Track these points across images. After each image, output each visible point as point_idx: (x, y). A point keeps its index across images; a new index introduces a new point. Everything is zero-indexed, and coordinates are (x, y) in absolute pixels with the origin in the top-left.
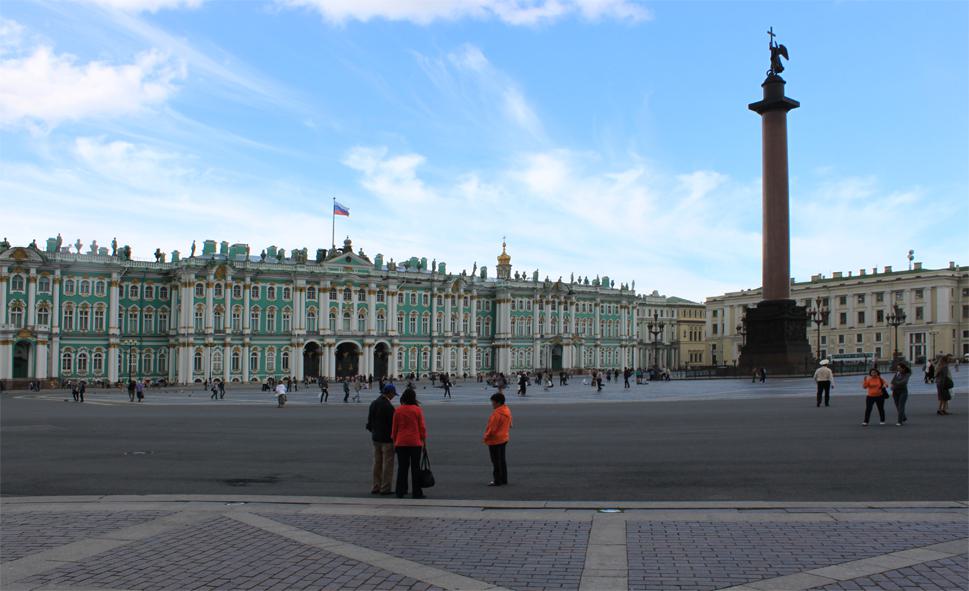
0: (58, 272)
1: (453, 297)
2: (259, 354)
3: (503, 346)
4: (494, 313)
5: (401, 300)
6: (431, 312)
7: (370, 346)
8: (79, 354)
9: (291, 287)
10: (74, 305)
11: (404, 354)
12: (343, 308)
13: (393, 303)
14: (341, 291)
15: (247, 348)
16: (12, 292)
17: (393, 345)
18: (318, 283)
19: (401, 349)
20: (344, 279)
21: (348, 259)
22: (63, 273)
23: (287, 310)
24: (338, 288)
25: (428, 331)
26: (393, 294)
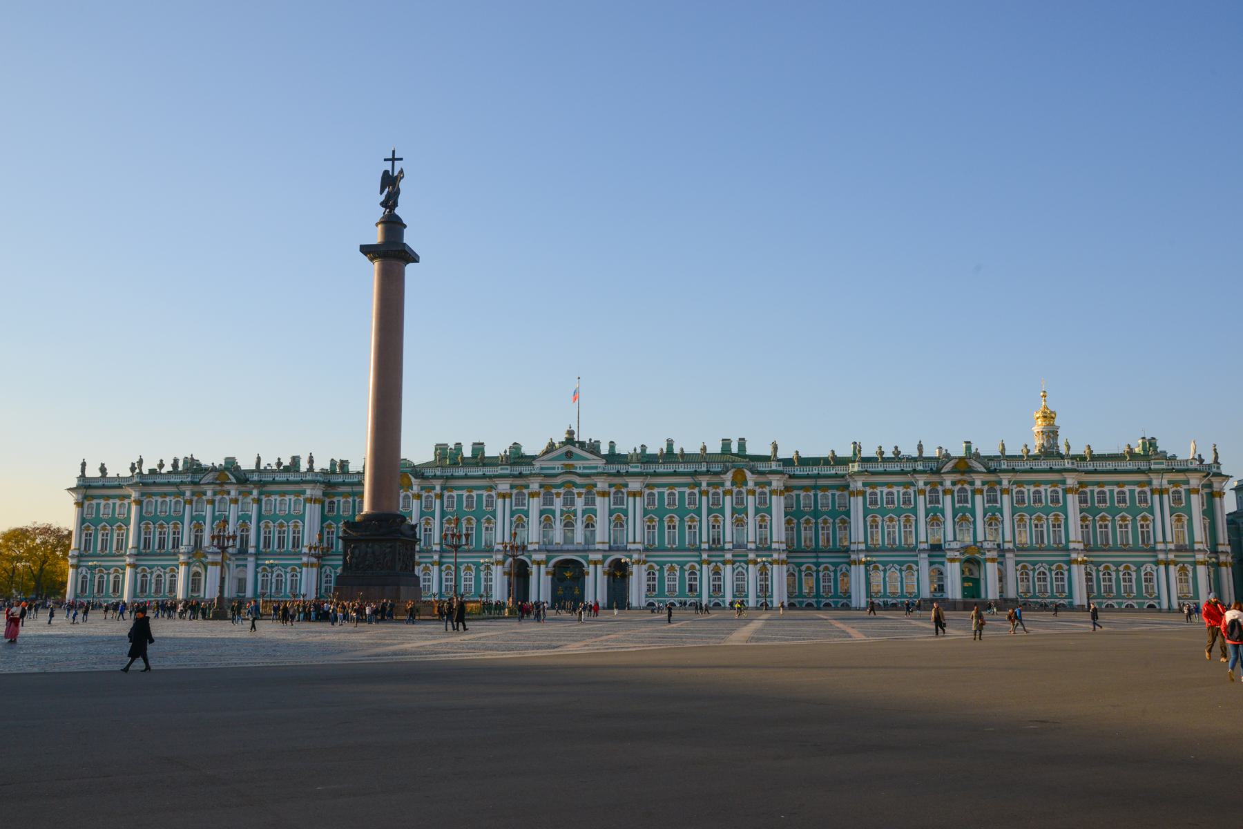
0: (255, 492)
1: (740, 493)
3: (854, 562)
4: (848, 513)
6: (700, 515)
7: (595, 563)
9: (493, 493)
10: (271, 524)
14: (558, 495)
15: (436, 568)
18: (527, 487)
19: (651, 567)
20: (558, 481)
21: (569, 455)
22: (261, 493)
23: (488, 521)
24: (554, 491)
26: (634, 495)
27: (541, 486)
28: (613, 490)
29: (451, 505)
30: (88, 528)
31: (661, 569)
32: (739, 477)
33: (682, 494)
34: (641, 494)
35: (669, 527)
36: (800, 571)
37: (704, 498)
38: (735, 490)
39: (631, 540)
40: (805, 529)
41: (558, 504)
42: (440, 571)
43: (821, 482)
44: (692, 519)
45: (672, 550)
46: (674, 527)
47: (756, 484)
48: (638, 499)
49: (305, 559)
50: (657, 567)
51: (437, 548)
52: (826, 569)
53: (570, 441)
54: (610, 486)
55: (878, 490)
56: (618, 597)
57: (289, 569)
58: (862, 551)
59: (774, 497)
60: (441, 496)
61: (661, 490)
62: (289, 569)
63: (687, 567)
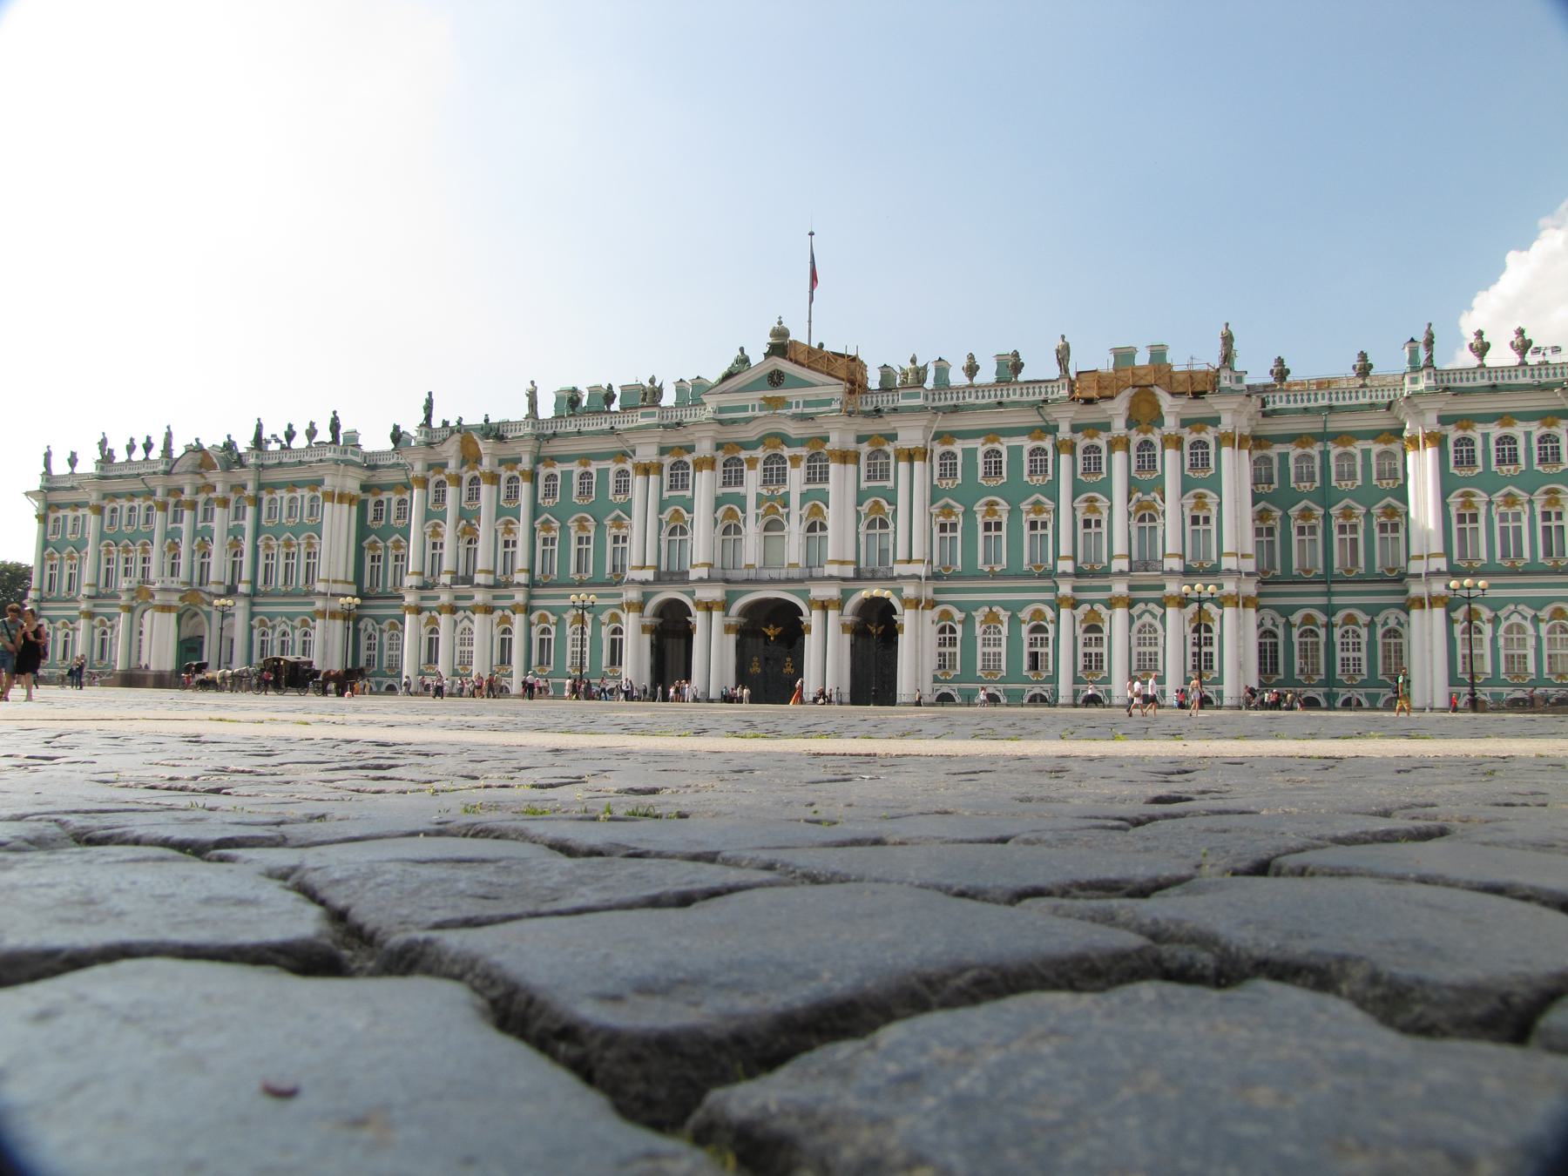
1: (1146, 445)
3: (1420, 603)
4: (1401, 493)
5: (948, 469)
7: (824, 606)
8: (278, 630)
9: (628, 466)
10: (274, 542)
11: (959, 628)
13: (912, 485)
14: (752, 463)
16: (200, 525)
18: (690, 449)
19: (946, 615)
23: (618, 522)
24: (743, 455)
25: (1050, 560)
26: (910, 456)
28: (865, 449)
30: (51, 556)
31: (968, 622)
32: (1145, 409)
33: (1015, 452)
34: (924, 454)
35: (987, 527)
36: (1289, 626)
37: (1065, 459)
38: (1136, 438)
40: (1301, 531)
41: (752, 482)
42: (529, 625)
43: (1338, 423)
44: (1038, 507)
45: (995, 576)
46: (998, 526)
47: (1184, 423)
48: (918, 465)
49: (320, 604)
50: (958, 615)
51: (521, 578)
52: (1350, 619)
53: (781, 346)
55: (1476, 433)
56: (873, 680)
57: (297, 622)
58: (1438, 573)
59: (1226, 452)
60: (532, 477)
62: (297, 622)
63: (1025, 614)
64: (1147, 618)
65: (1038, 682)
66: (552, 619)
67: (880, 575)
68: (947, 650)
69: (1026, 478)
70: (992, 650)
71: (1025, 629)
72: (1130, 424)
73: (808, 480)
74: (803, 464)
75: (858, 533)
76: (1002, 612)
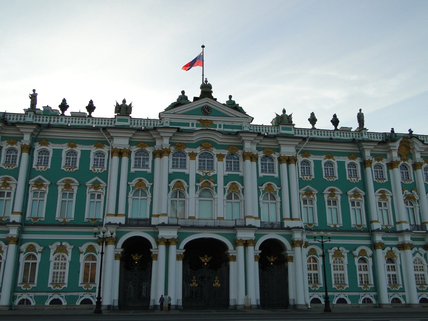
1: (404, 167)
2: (39, 256)
7: (246, 244)
9: (105, 150)
12: (198, 181)
14: (193, 156)
15: (12, 247)
17: (293, 244)
18: (153, 144)
19: (313, 251)
20: (195, 138)
21: (206, 110)
23: (96, 185)
24: (187, 151)
25: (365, 223)
26: (289, 160)
27: (172, 144)
28: (261, 154)
29: (43, 161)
37: (368, 170)
39: (287, 215)
41: (192, 167)
42: (18, 252)
46: (335, 203)
48: (292, 166)
54: (258, 149)
61: (318, 158)
63: (356, 252)
64: (418, 255)
65: (366, 291)
66: (39, 248)
67: (276, 226)
68: (313, 272)
69: (348, 179)
70: (339, 272)
71: (356, 260)
72: (399, 155)
73: (227, 169)
74: (225, 159)
75: (259, 201)
76: (345, 250)
